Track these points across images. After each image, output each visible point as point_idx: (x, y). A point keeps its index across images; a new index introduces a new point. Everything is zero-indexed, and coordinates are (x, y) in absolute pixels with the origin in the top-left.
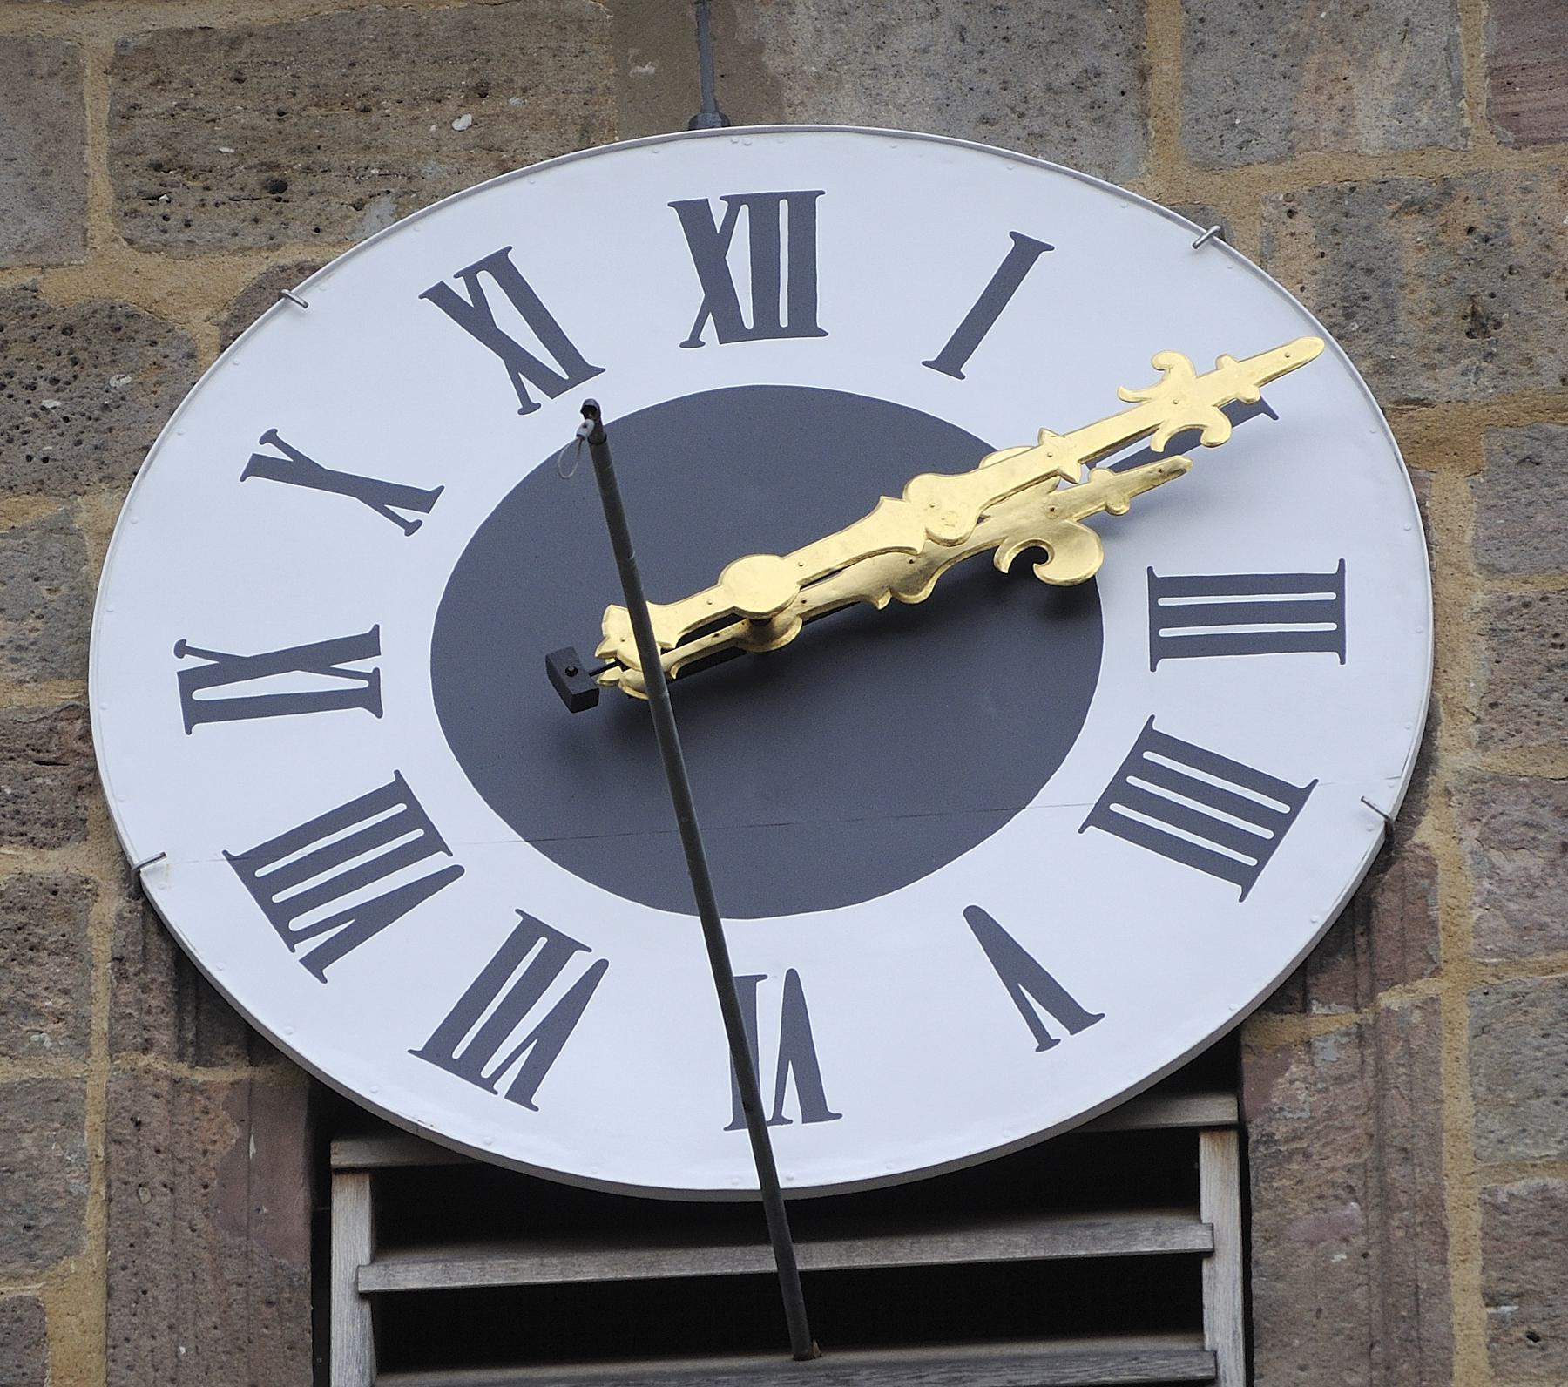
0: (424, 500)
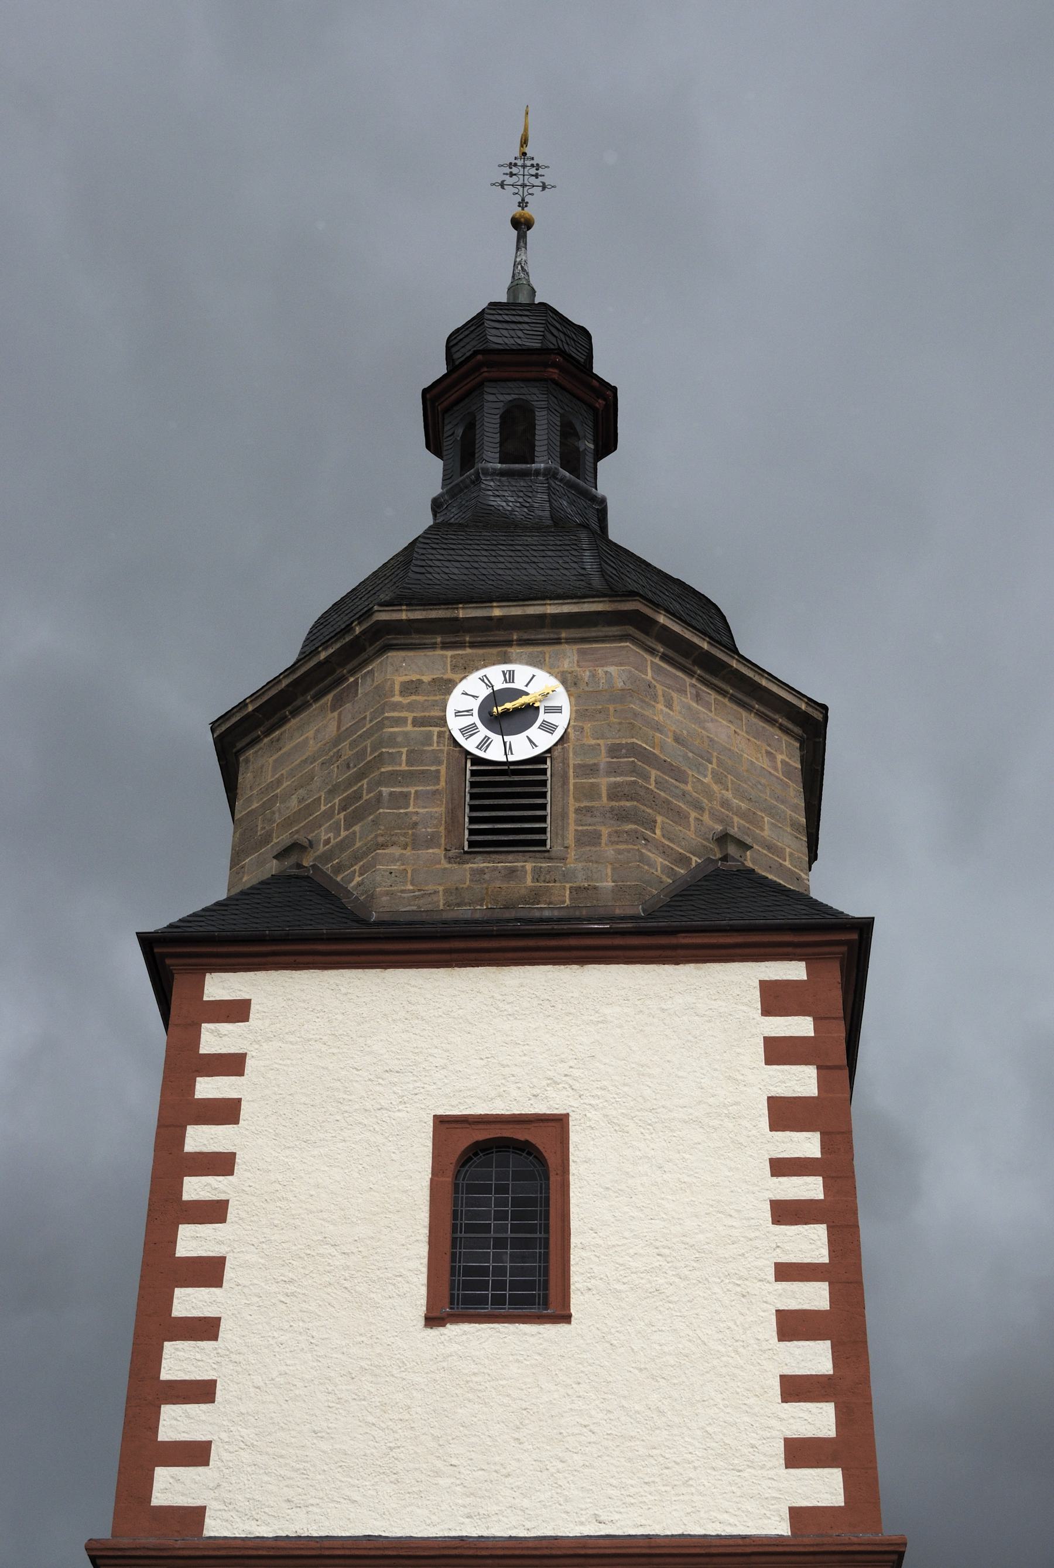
0: (477, 697)
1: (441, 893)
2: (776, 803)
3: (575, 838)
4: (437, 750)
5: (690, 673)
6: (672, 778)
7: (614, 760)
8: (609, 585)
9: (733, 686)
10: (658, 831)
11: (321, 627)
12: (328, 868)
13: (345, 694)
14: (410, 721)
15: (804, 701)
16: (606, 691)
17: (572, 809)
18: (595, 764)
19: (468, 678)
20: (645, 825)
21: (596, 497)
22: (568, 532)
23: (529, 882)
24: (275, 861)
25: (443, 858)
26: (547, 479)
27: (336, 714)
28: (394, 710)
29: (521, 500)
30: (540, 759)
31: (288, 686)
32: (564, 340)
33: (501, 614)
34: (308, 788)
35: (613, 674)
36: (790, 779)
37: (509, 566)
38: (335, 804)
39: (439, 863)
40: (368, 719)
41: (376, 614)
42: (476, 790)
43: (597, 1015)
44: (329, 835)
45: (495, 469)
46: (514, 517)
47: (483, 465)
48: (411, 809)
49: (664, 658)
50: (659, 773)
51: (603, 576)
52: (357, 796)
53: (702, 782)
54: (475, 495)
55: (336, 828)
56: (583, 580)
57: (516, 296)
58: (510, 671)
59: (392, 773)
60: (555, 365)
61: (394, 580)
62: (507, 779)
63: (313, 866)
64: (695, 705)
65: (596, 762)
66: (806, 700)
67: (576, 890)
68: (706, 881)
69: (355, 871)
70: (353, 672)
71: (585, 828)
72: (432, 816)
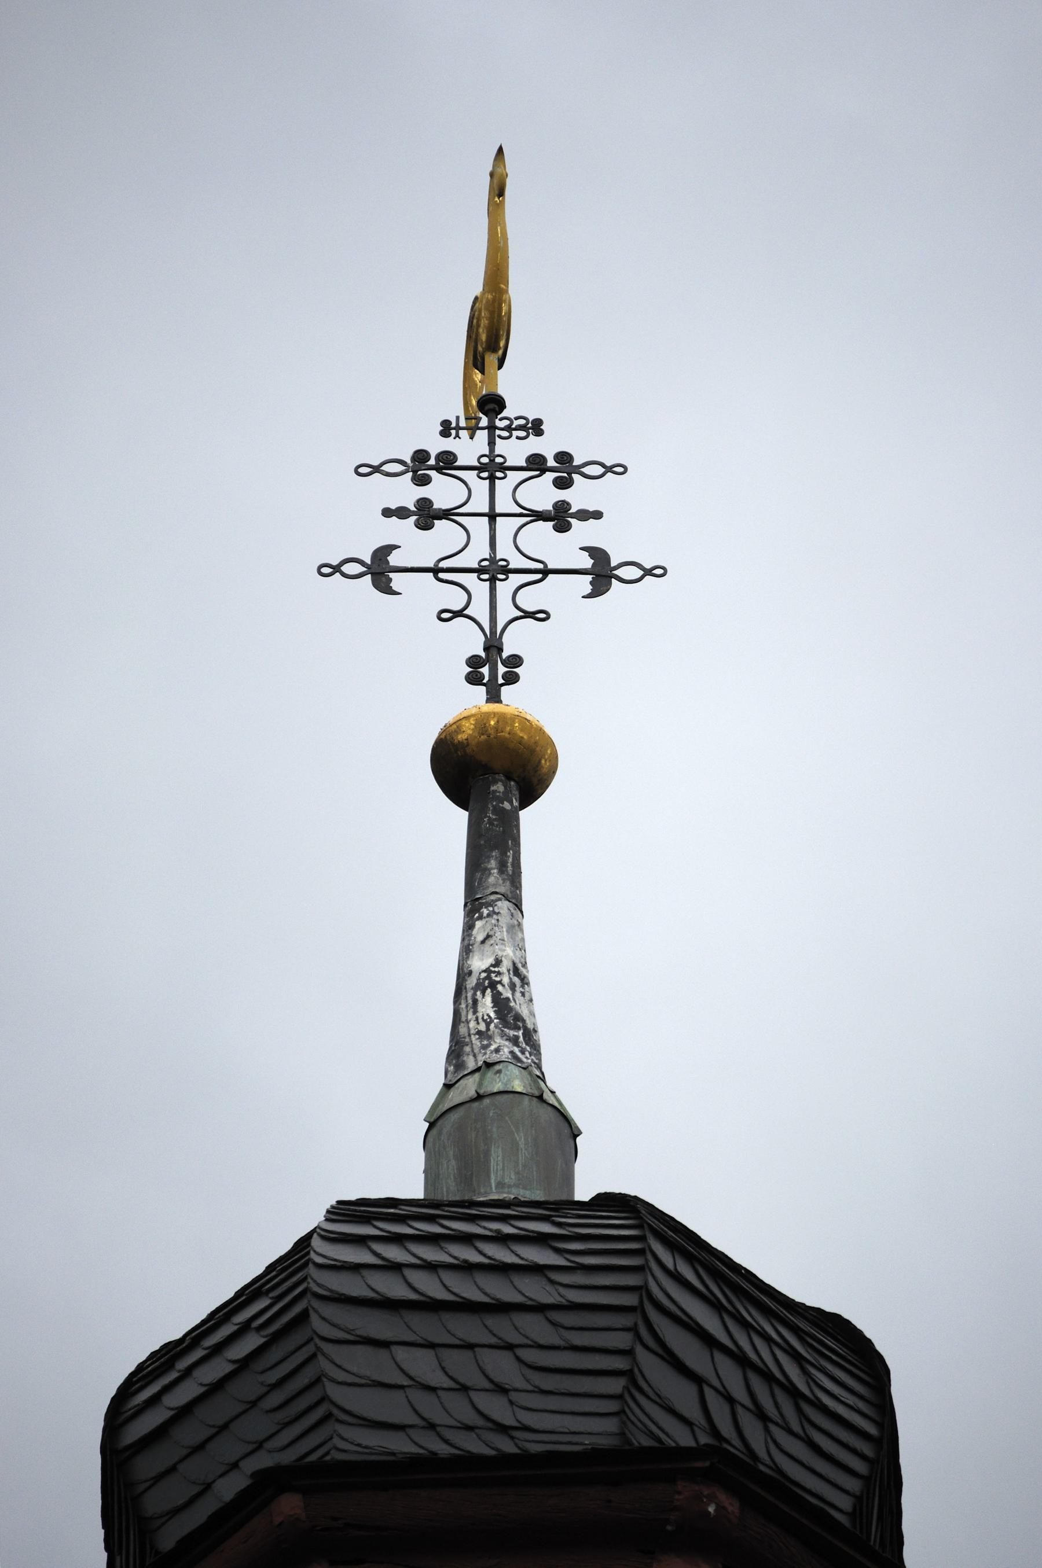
32: (739, 1393)
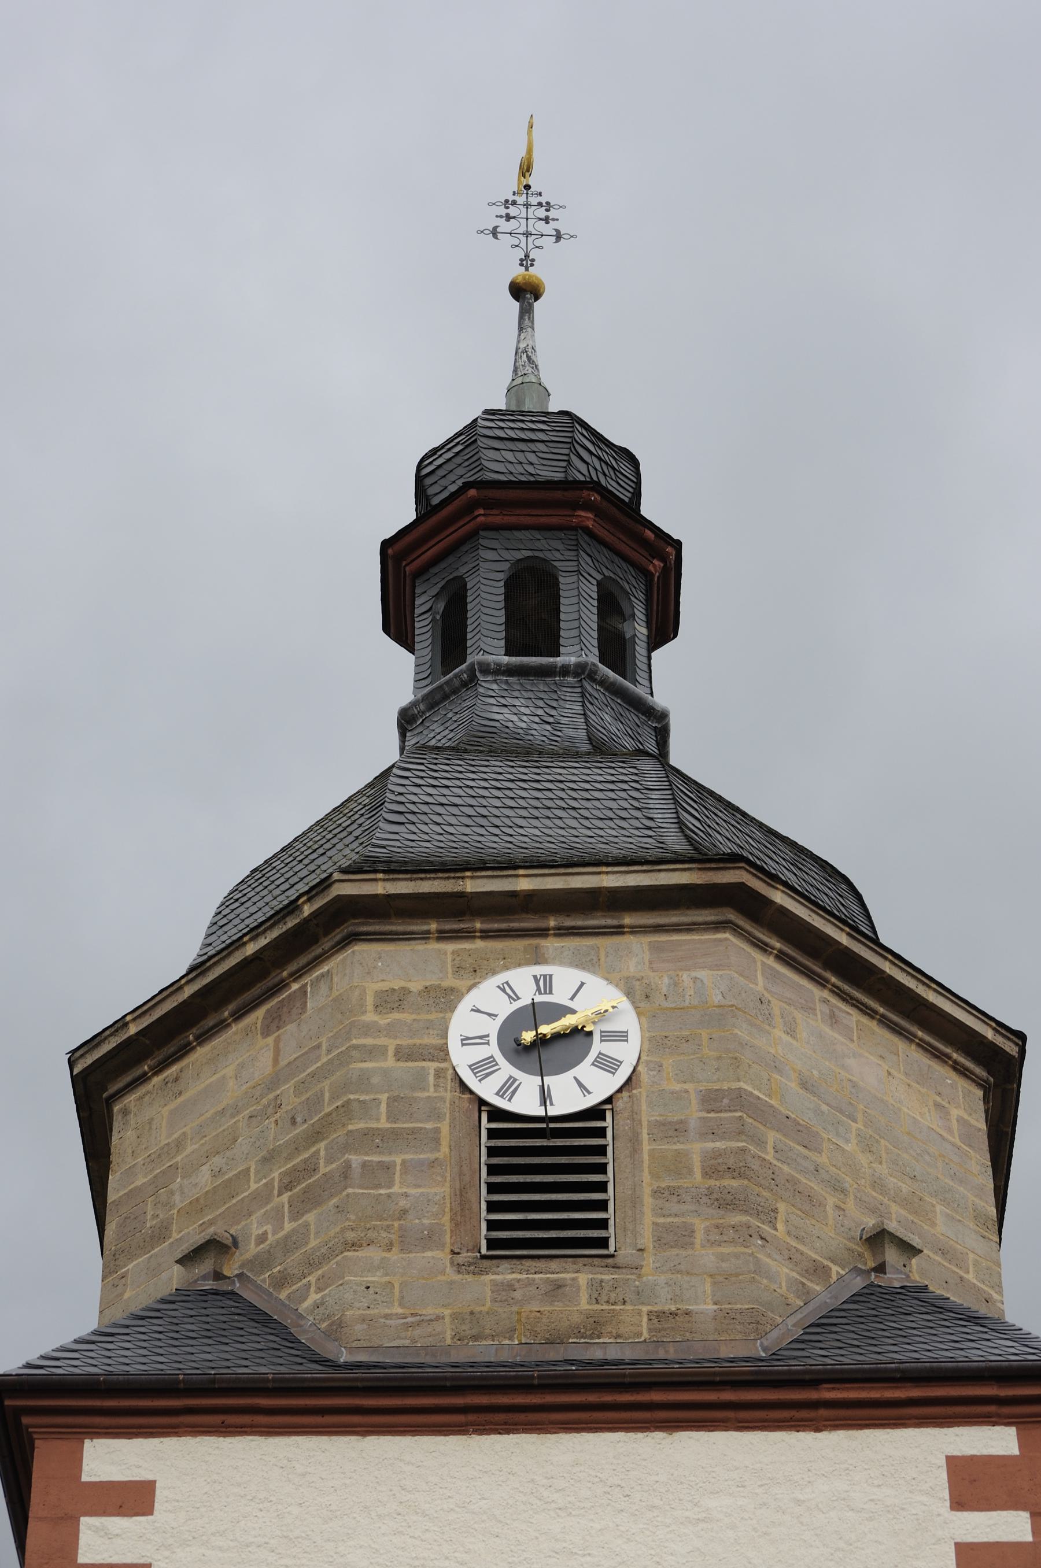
0: (496, 1016)
1: (447, 1320)
2: (951, 1183)
3: (653, 1236)
4: (435, 1097)
5: (821, 982)
6: (799, 1144)
7: (712, 1115)
8: (692, 845)
9: (884, 1002)
10: (780, 1226)
11: (237, 904)
12: (263, 1279)
13: (285, 1009)
14: (391, 1052)
15: (991, 1026)
16: (695, 1007)
17: (647, 1191)
18: (681, 1122)
19: (481, 986)
20: (762, 1216)
21: (654, 709)
22: (623, 762)
23: (584, 1304)
24: (177, 1268)
25: (448, 1265)
26: (581, 680)
27: (270, 1040)
28: (366, 1035)
29: (540, 712)
30: (596, 1112)
31: (192, 996)
32: (599, 468)
33: (531, 887)
34: (228, 1153)
35: (705, 981)
36: (970, 1146)
37: (535, 813)
38: (273, 1179)
39: (443, 1272)
40: (324, 1048)
41: (336, 885)
42: (496, 1161)
43: (696, 1509)
44: (265, 1228)
45: (499, 665)
46: (531, 738)
47: (480, 657)
48: (396, 1189)
49: (782, 957)
50: (779, 1136)
51: (683, 831)
52: (310, 1168)
53: (843, 1150)
54: (468, 703)
55: (277, 1217)
56: (650, 837)
57: (520, 401)
58: (545, 976)
59: (366, 1133)
60: (588, 506)
61: (355, 834)
62: (545, 1144)
63: (240, 1276)
64: (827, 1030)
65: (683, 1118)
66: (994, 1025)
67: (659, 1316)
68: (855, 1302)
69: (309, 1284)
70: (297, 975)
71: (669, 1220)
72: (429, 1200)
